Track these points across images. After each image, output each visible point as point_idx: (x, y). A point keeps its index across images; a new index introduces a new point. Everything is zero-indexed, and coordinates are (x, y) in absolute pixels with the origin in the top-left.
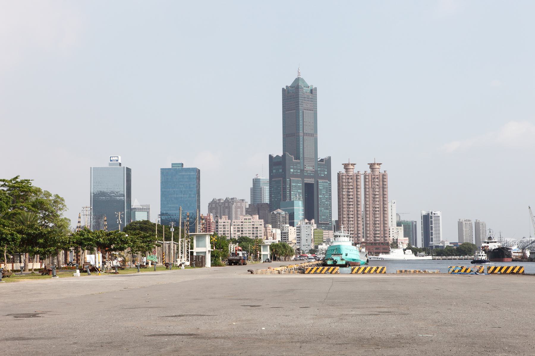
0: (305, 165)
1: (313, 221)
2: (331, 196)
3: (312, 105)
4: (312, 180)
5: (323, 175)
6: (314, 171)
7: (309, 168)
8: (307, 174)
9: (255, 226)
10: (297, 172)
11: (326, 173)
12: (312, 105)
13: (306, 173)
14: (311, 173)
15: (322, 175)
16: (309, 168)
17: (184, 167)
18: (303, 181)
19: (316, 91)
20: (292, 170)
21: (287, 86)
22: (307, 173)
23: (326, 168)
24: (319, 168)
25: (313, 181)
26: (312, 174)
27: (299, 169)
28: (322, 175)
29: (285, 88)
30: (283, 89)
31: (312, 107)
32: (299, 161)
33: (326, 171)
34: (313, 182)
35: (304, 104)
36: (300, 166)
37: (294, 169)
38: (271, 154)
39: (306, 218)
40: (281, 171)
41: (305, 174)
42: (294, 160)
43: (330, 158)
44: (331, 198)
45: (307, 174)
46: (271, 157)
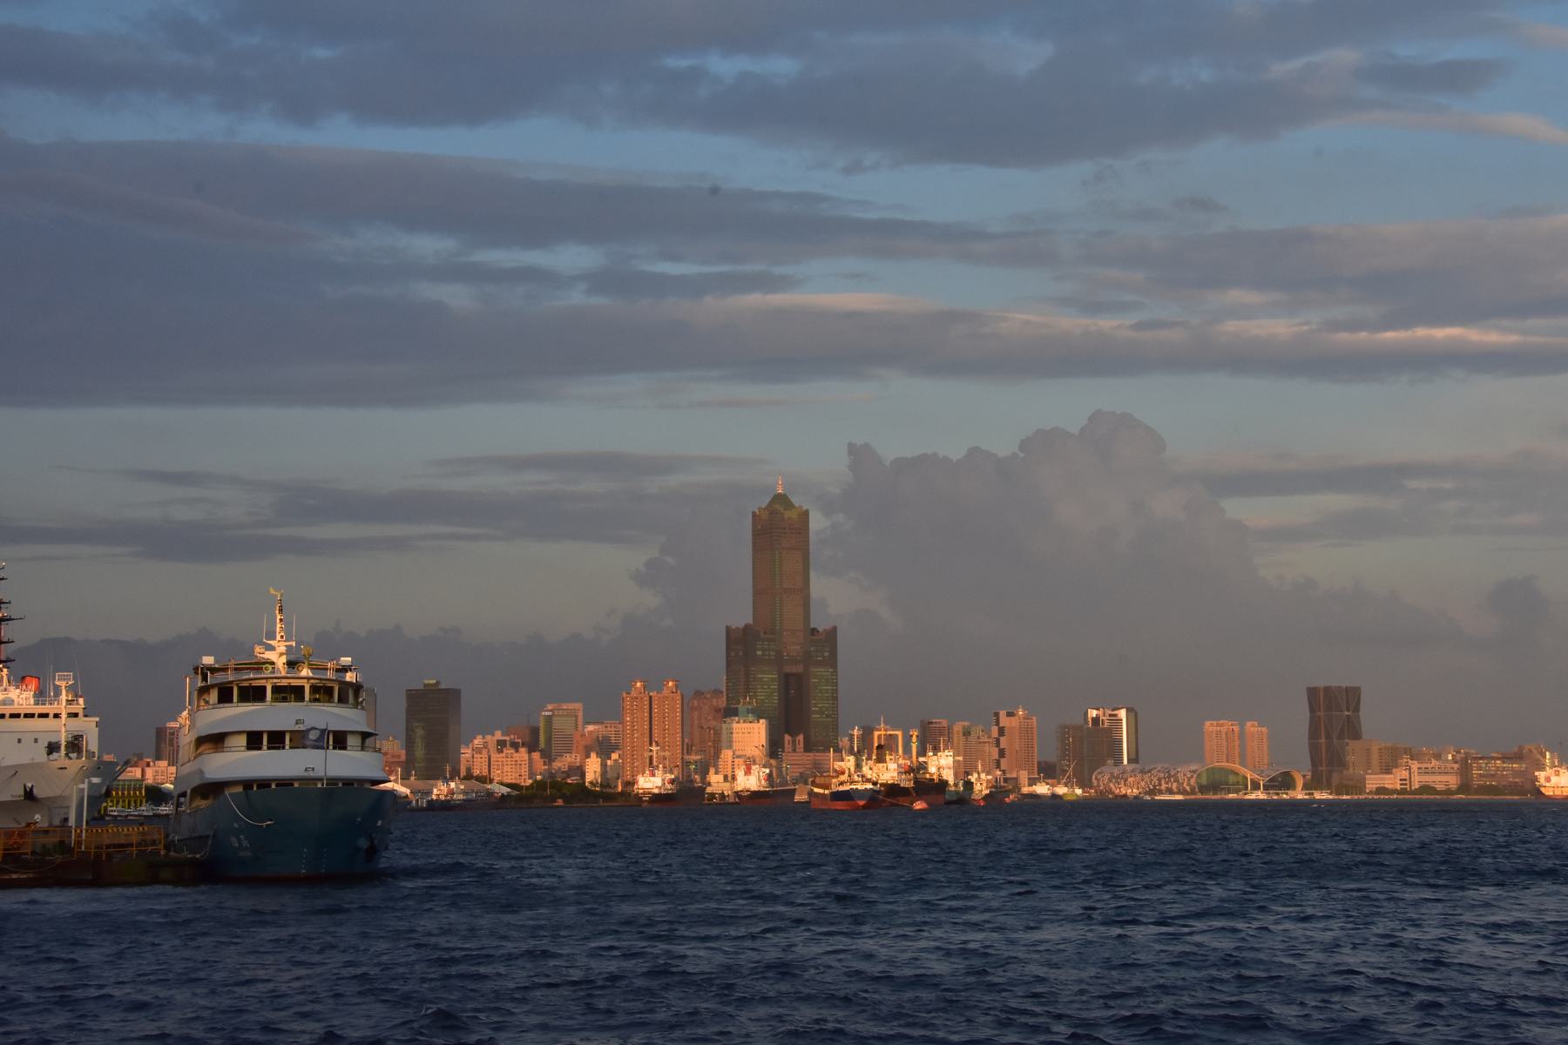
2: (837, 693)
7: (793, 648)
9: (519, 762)
10: (769, 655)
11: (826, 654)
16: (793, 648)
17: (443, 686)
19: (808, 515)
20: (759, 653)
21: (760, 509)
29: (757, 511)
30: (754, 514)
32: (772, 636)
37: (763, 650)
38: (729, 624)
39: (787, 733)
40: (741, 653)
42: (762, 635)
43: (835, 629)
44: (837, 697)
46: (728, 629)
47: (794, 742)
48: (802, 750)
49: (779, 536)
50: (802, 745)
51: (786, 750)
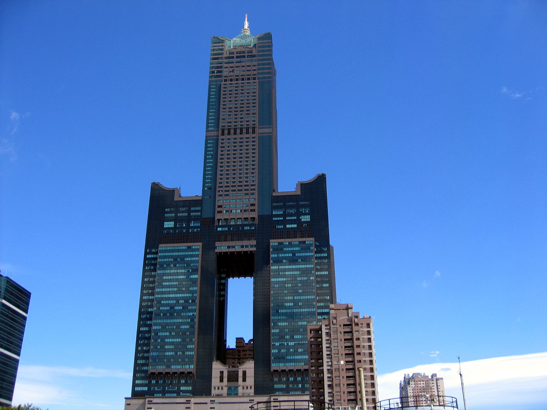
0: (220, 206)
1: (249, 367)
3: (255, 68)
4: (245, 243)
5: (295, 226)
6: (253, 219)
8: (226, 229)
10: (188, 227)
11: (306, 218)
12: (255, 68)
13: (222, 226)
14: (243, 226)
15: (288, 226)
18: (208, 248)
20: (169, 225)
22: (229, 226)
23: (304, 206)
24: (277, 208)
25: (252, 246)
26: (250, 225)
27: (196, 219)
28: (288, 226)
33: (305, 214)
34: (254, 249)
35: (224, 70)
36: (200, 211)
37: (176, 220)
41: (219, 229)
43: (321, 180)
45: (226, 229)
47: (233, 377)
48: (252, 391)
49: (221, 67)
50: (250, 381)
51: (214, 392)
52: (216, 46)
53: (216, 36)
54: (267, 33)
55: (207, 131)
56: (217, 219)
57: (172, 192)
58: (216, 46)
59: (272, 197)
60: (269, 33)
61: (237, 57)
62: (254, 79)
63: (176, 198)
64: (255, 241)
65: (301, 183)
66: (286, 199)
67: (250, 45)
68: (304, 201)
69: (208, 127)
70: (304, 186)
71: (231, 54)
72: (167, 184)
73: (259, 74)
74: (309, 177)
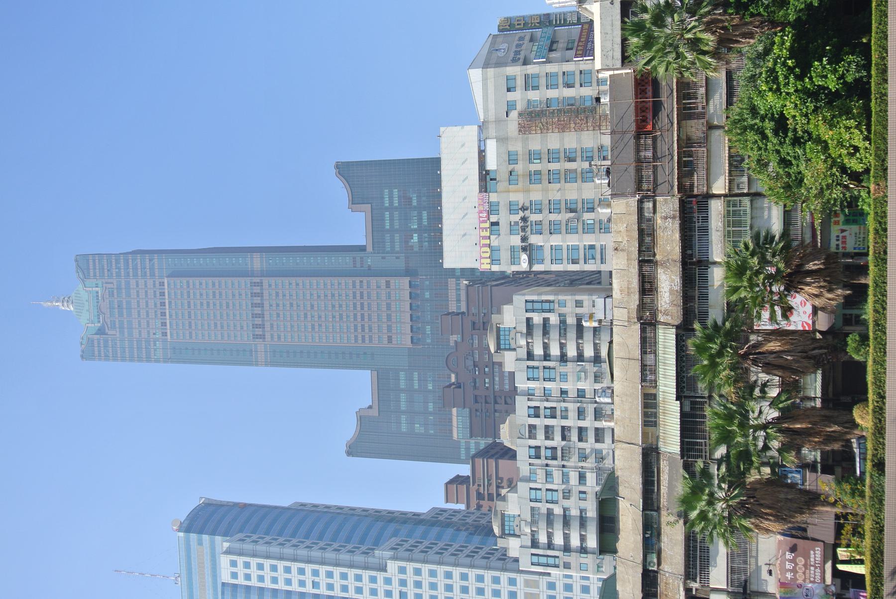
31: (150, 283)
43: (345, 170)
52: (99, 351)
53: (80, 353)
54: (74, 264)
55: (257, 365)
56: (412, 342)
57: (362, 419)
58: (99, 351)
59: (375, 253)
60: (76, 261)
61: (121, 314)
62: (162, 284)
63: (375, 412)
64: (449, 279)
65: (351, 203)
66: (376, 226)
67: (97, 292)
68: (382, 198)
69: (249, 363)
70: (355, 201)
71: (115, 326)
72: (349, 430)
73: (153, 275)
74: (340, 191)
